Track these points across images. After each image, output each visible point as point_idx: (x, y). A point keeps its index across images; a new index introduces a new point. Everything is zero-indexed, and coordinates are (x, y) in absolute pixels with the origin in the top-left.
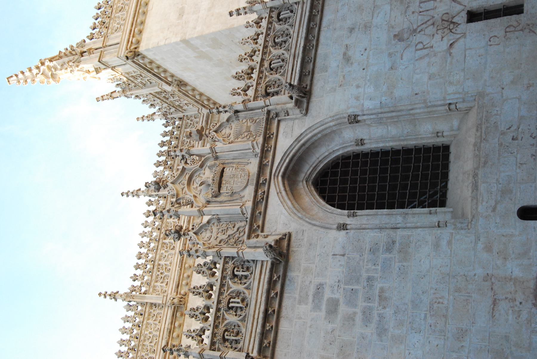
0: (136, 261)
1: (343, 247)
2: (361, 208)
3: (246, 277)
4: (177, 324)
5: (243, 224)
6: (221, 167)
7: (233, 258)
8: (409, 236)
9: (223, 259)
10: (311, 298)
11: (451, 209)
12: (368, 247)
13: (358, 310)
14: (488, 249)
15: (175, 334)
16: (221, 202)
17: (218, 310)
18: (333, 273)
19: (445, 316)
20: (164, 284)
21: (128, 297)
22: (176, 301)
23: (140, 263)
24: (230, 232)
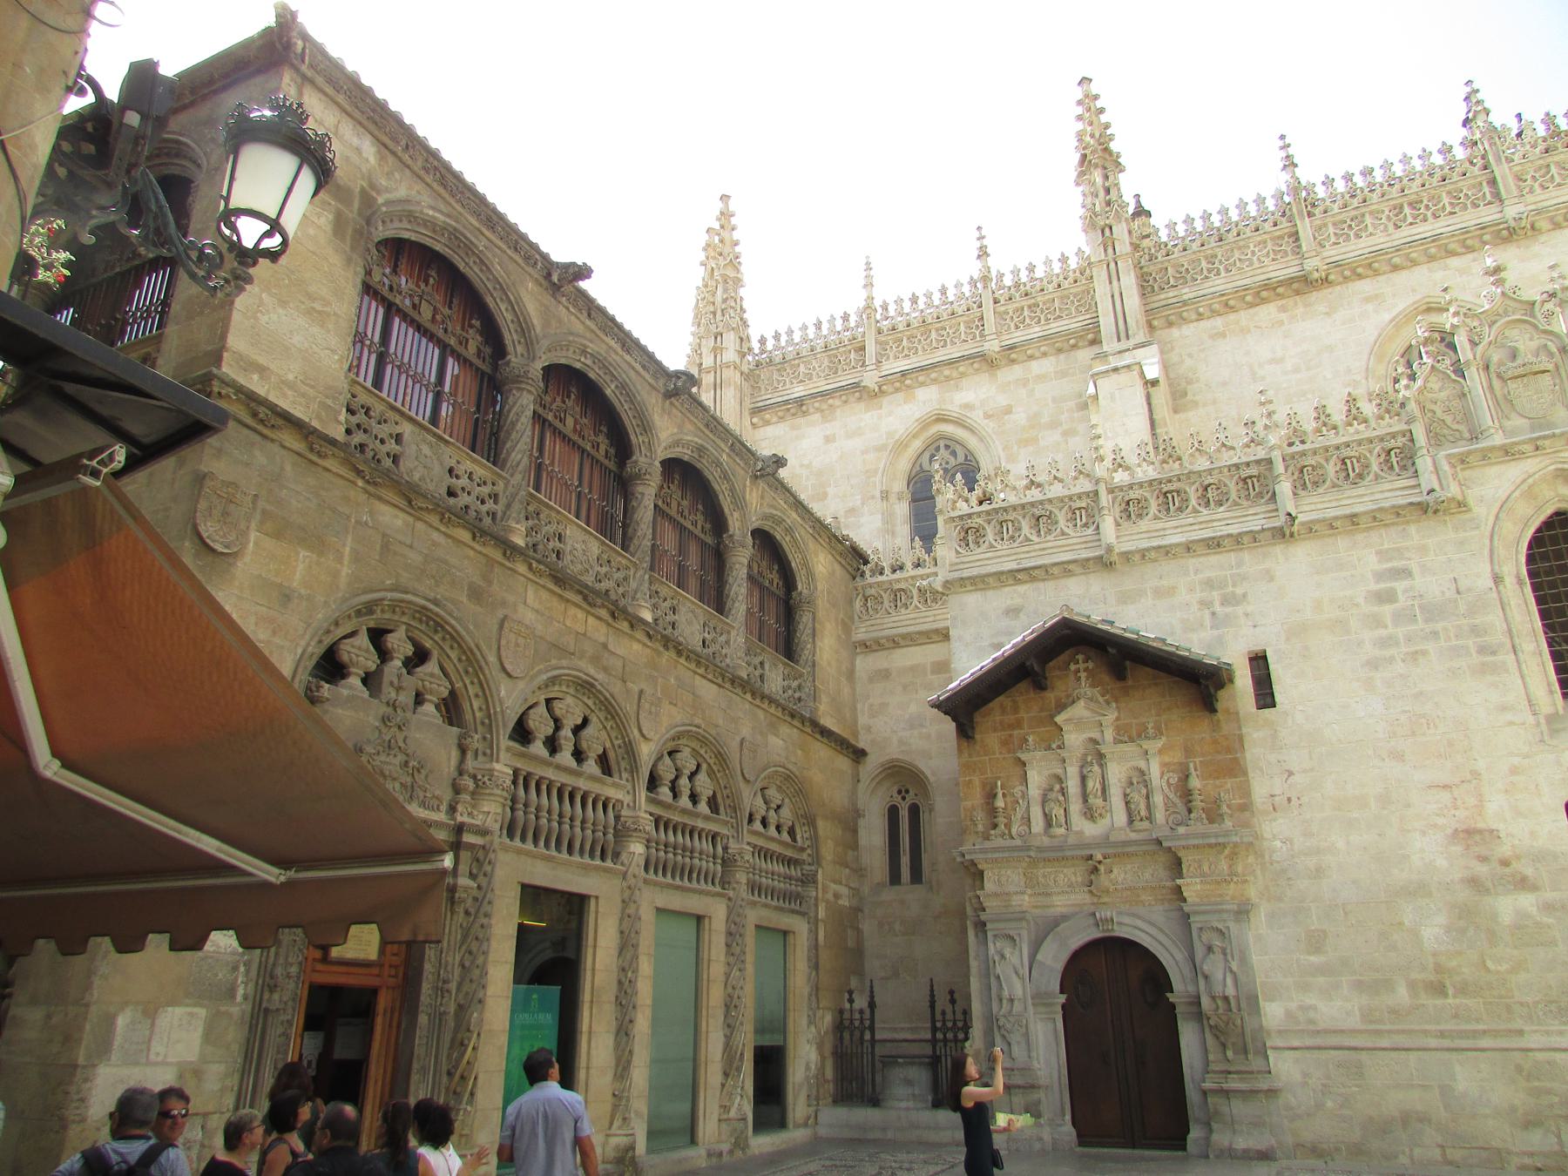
0: (1356, 170)
1: (1469, 590)
2: (1535, 588)
3: (1392, 468)
4: (1280, 290)
5: (1467, 435)
6: (1550, 367)
7: (1412, 440)
8: (1507, 671)
9: (1406, 427)
10: (1389, 565)
11: (1561, 712)
12: (1477, 621)
13: (1391, 630)
14: (1514, 771)
15: (1264, 294)
16: (1491, 387)
17: (1338, 448)
18: (1432, 586)
19: (1414, 734)
20: (1333, 239)
21: (1296, 187)
22: (1316, 275)
23: (1355, 179)
24: (1448, 420)
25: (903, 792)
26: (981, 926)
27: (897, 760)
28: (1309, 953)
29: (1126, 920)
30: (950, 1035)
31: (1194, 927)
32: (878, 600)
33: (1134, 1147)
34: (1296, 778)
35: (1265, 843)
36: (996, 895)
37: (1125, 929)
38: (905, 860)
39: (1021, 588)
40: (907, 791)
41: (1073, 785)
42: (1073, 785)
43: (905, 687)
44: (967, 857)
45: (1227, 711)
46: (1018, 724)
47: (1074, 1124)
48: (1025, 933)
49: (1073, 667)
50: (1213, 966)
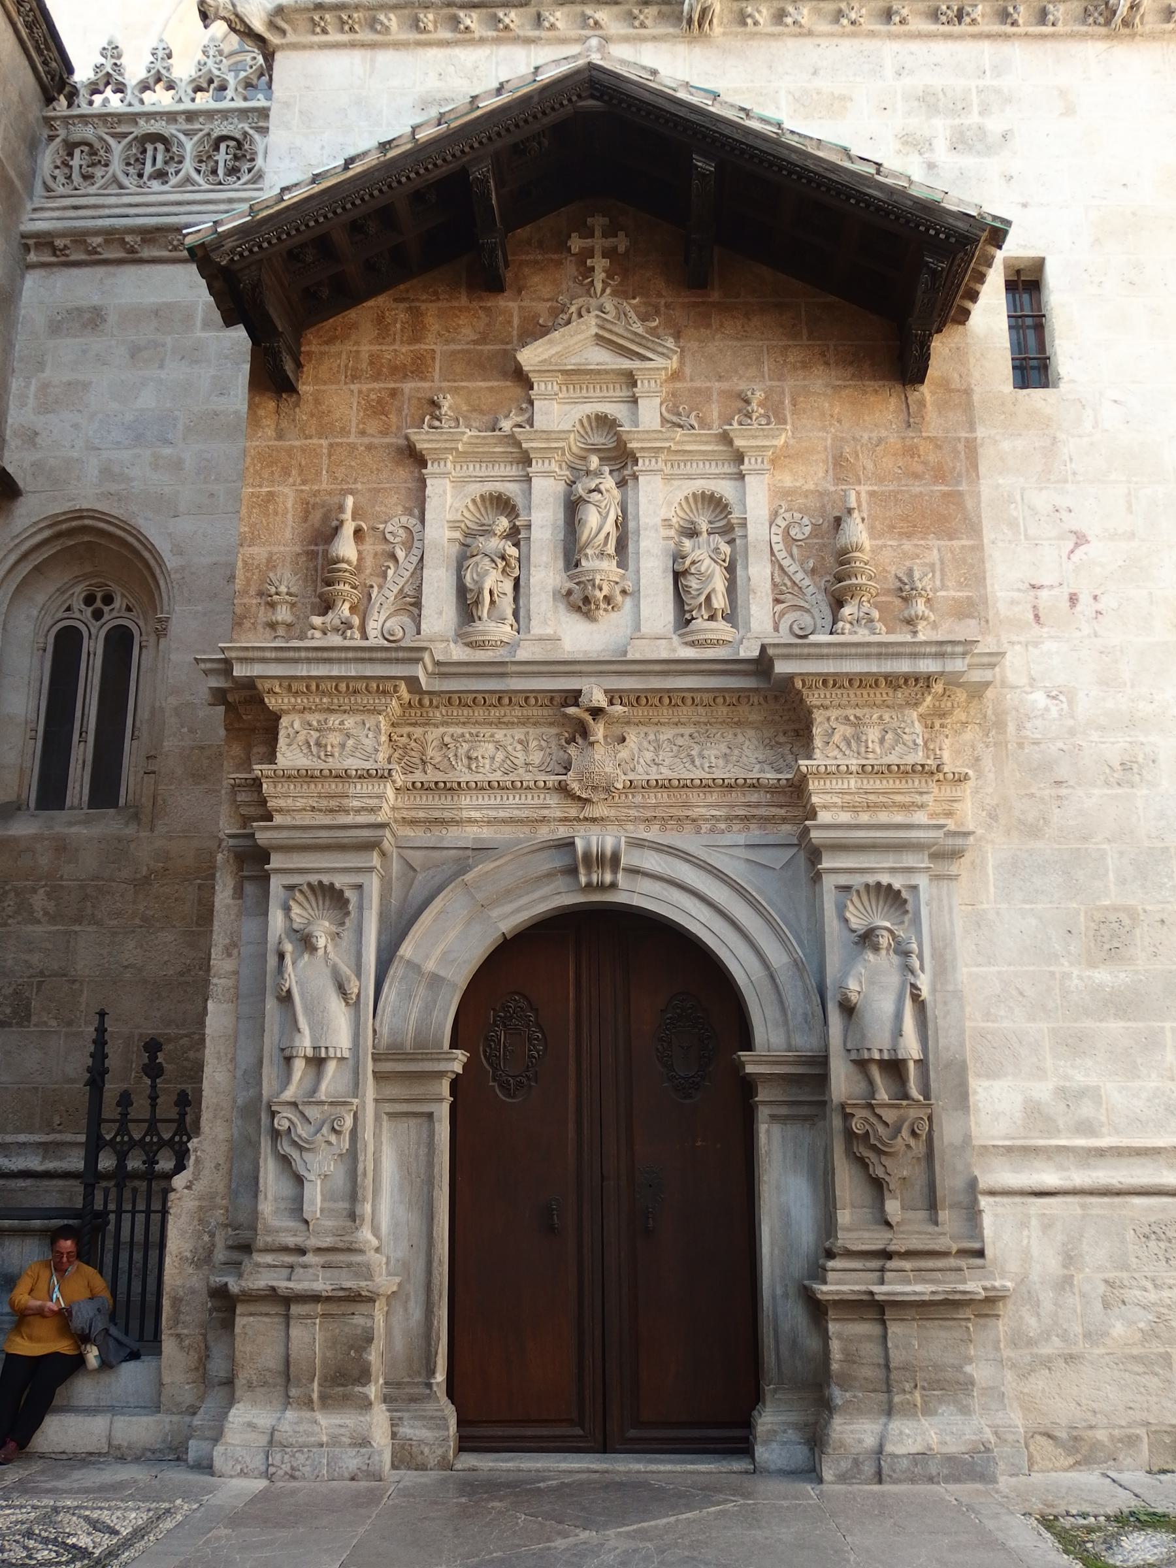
25: (98, 601)
26: (253, 861)
27: (94, 514)
28: (1092, 965)
29: (652, 862)
30: (134, 1163)
31: (829, 882)
32: (96, 155)
33: (604, 1448)
34: (1092, 550)
35: (1011, 698)
36: (308, 776)
37: (646, 885)
38: (82, 754)
39: (467, 56)
40: (108, 600)
41: (544, 521)
42: (544, 521)
43: (135, 352)
44: (239, 671)
45: (945, 384)
46: (418, 367)
47: (450, 1394)
48: (374, 885)
49: (576, 244)
50: (873, 984)
